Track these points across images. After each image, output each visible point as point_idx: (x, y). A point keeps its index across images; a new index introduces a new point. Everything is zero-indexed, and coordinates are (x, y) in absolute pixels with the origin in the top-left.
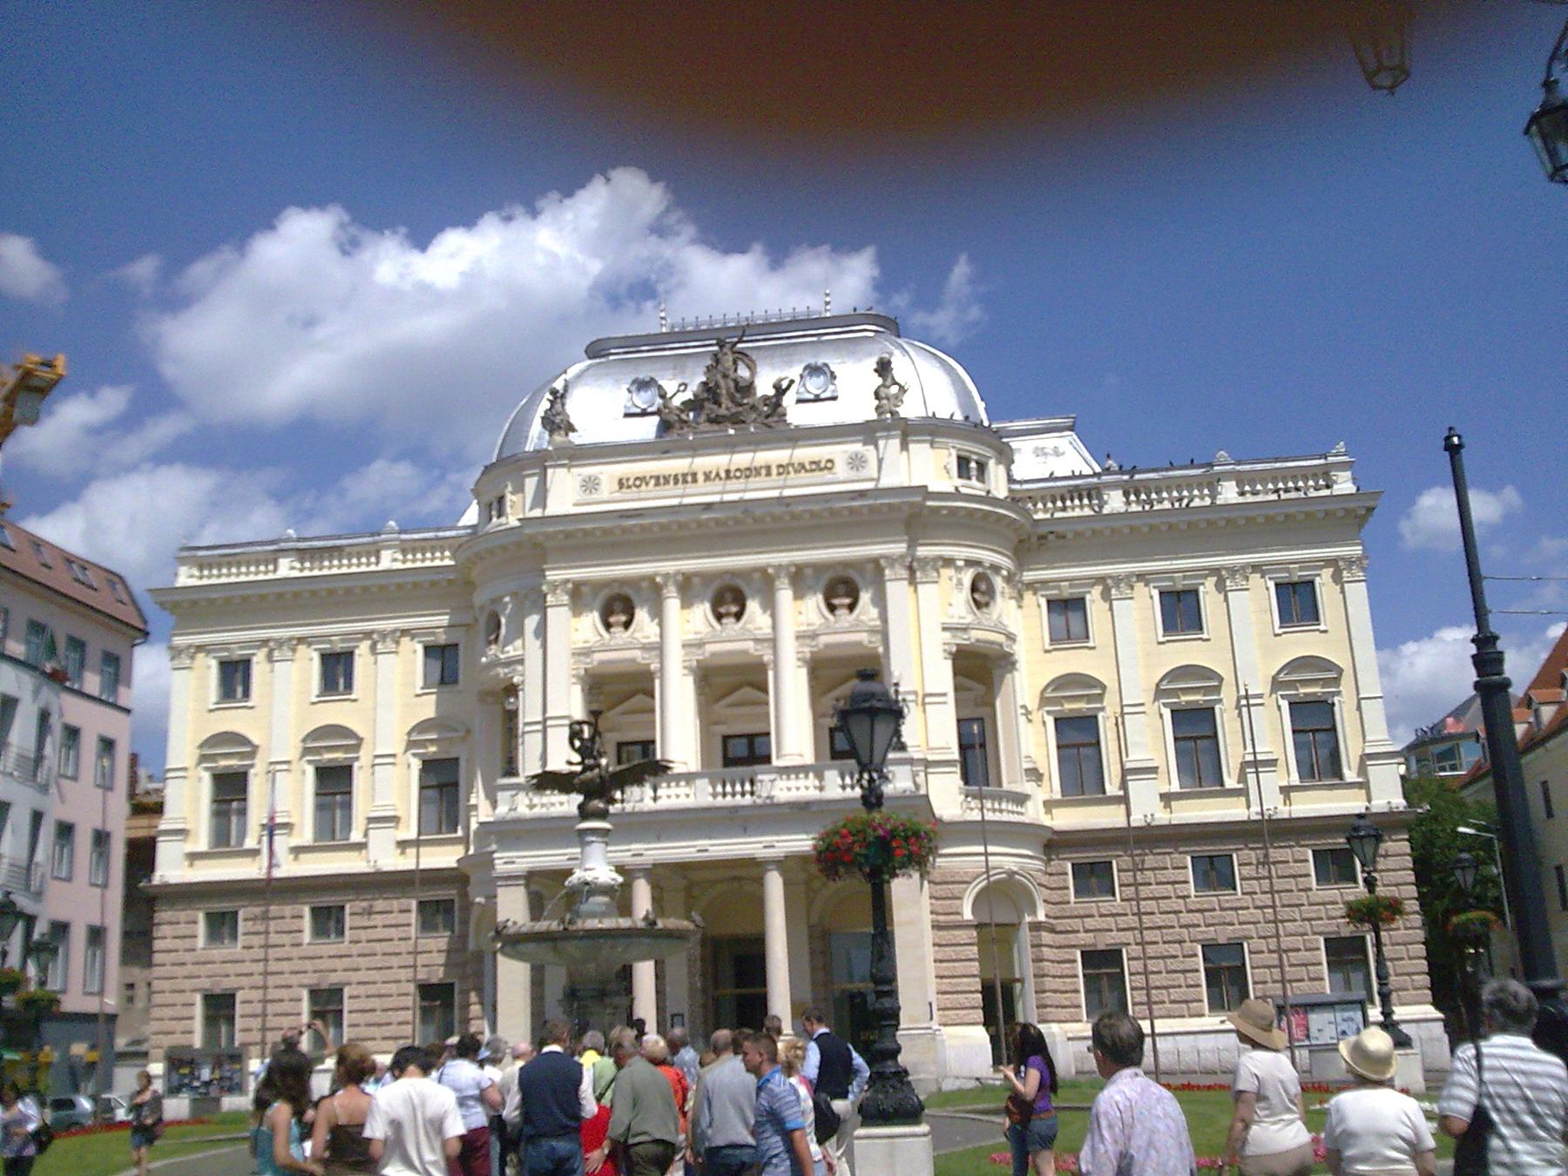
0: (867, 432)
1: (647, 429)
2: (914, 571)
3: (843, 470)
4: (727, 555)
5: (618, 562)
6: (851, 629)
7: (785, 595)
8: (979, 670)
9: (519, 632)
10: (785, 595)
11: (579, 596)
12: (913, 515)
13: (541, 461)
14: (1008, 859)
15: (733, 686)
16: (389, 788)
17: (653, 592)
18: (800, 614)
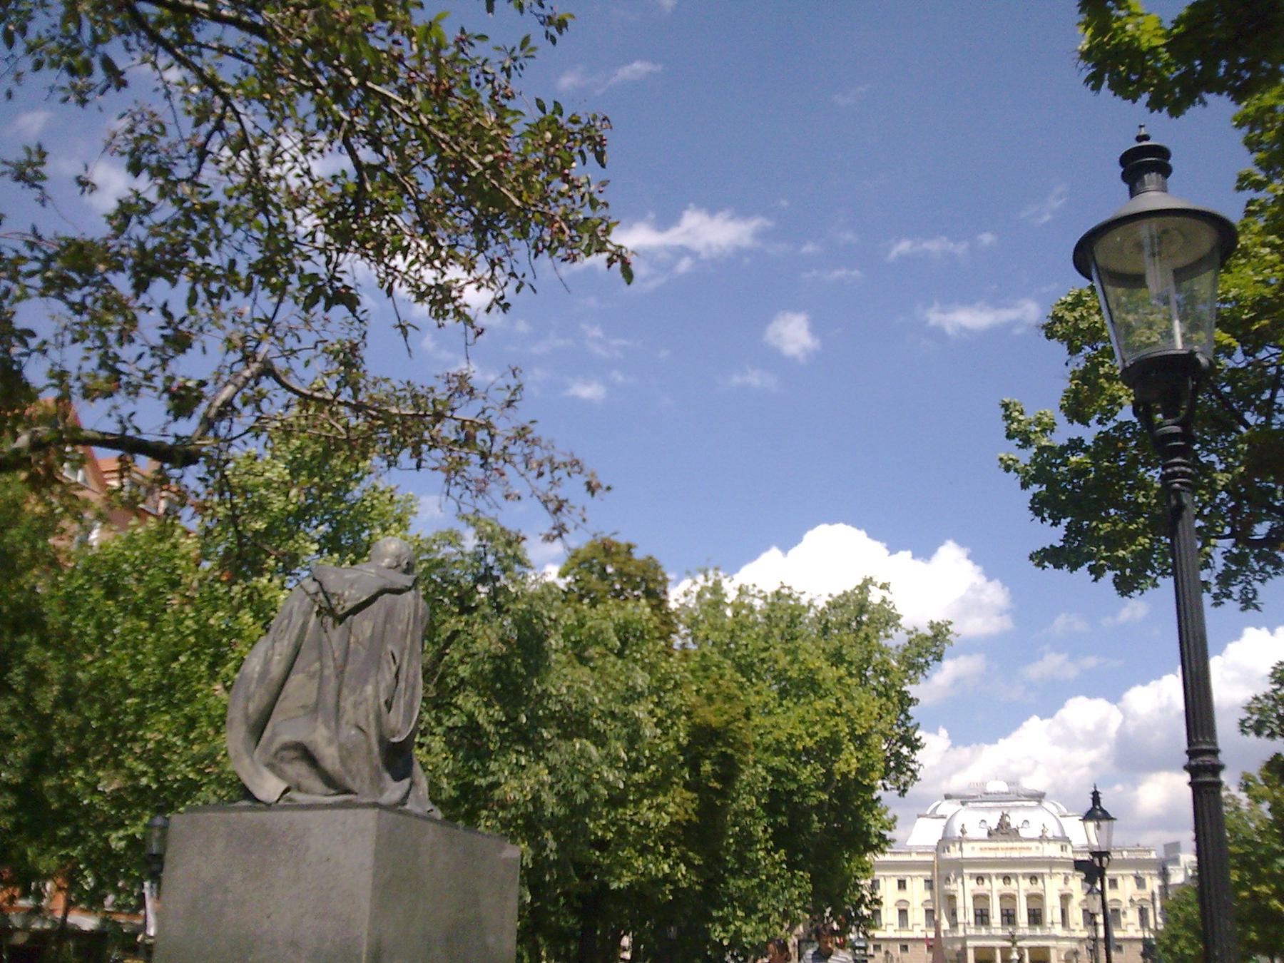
0: (1042, 839)
1: (984, 835)
2: (1051, 875)
3: (1035, 851)
4: (1007, 869)
5: (980, 869)
6: (1037, 888)
7: (1020, 879)
8: (1065, 898)
9: (955, 881)
10: (1020, 879)
11: (971, 876)
12: (1051, 863)
13: (961, 840)
14: (1074, 945)
15: (1008, 898)
16: (917, 916)
17: (989, 876)
18: (1025, 884)
